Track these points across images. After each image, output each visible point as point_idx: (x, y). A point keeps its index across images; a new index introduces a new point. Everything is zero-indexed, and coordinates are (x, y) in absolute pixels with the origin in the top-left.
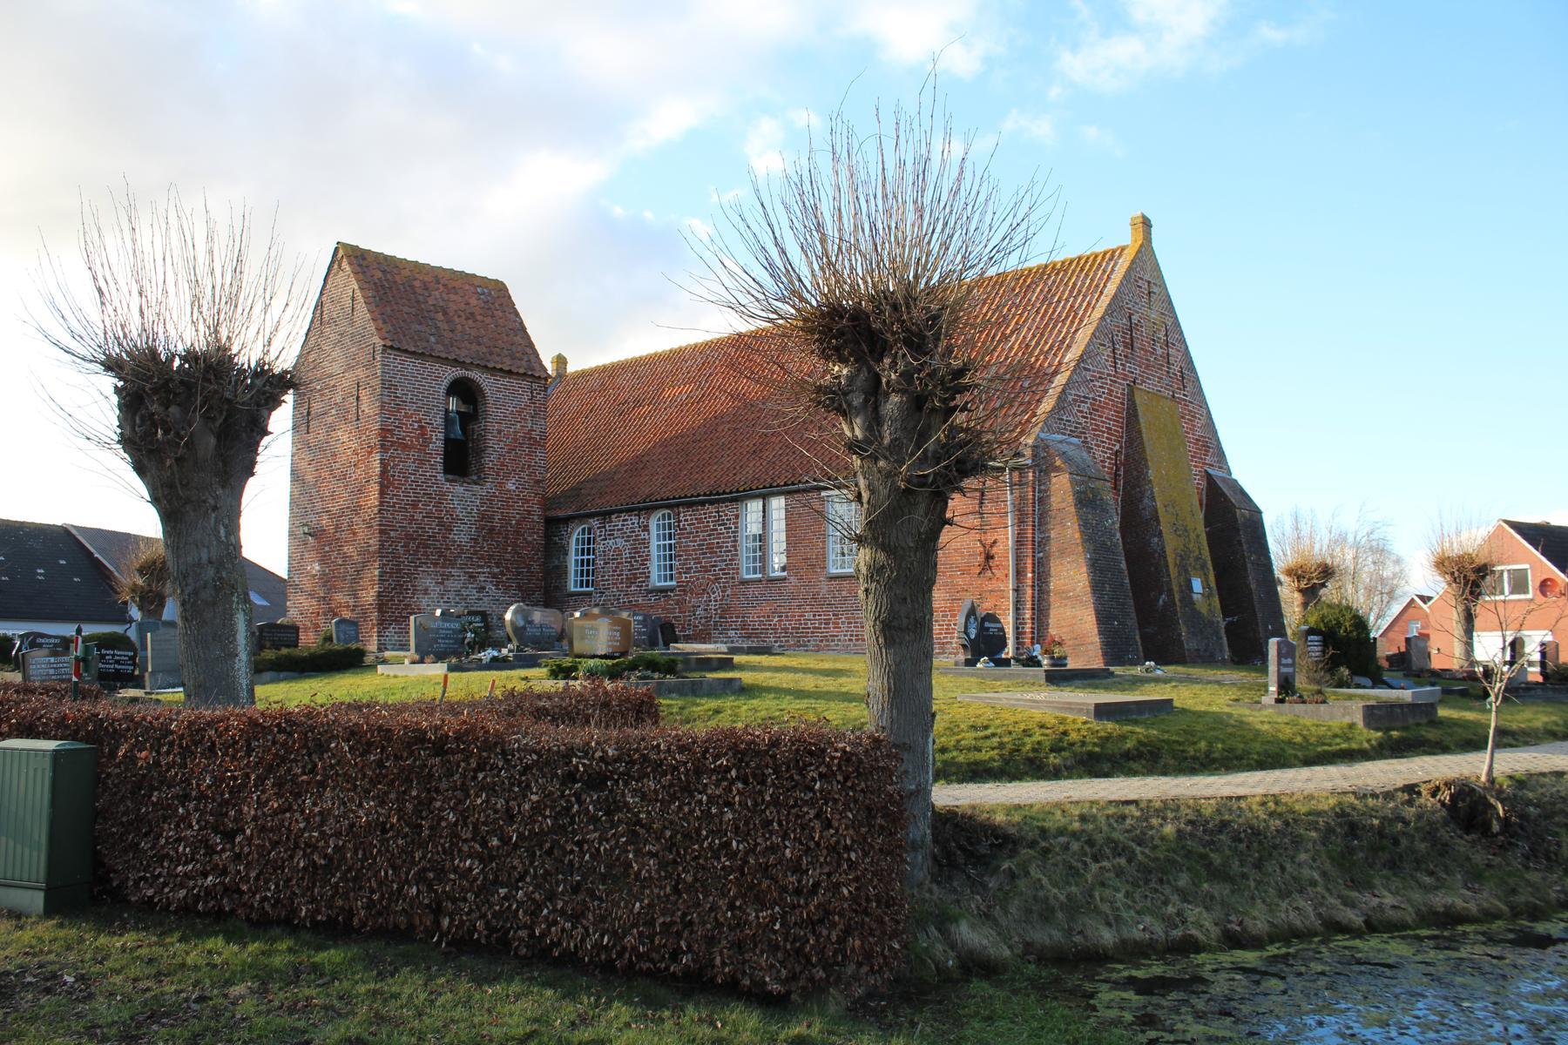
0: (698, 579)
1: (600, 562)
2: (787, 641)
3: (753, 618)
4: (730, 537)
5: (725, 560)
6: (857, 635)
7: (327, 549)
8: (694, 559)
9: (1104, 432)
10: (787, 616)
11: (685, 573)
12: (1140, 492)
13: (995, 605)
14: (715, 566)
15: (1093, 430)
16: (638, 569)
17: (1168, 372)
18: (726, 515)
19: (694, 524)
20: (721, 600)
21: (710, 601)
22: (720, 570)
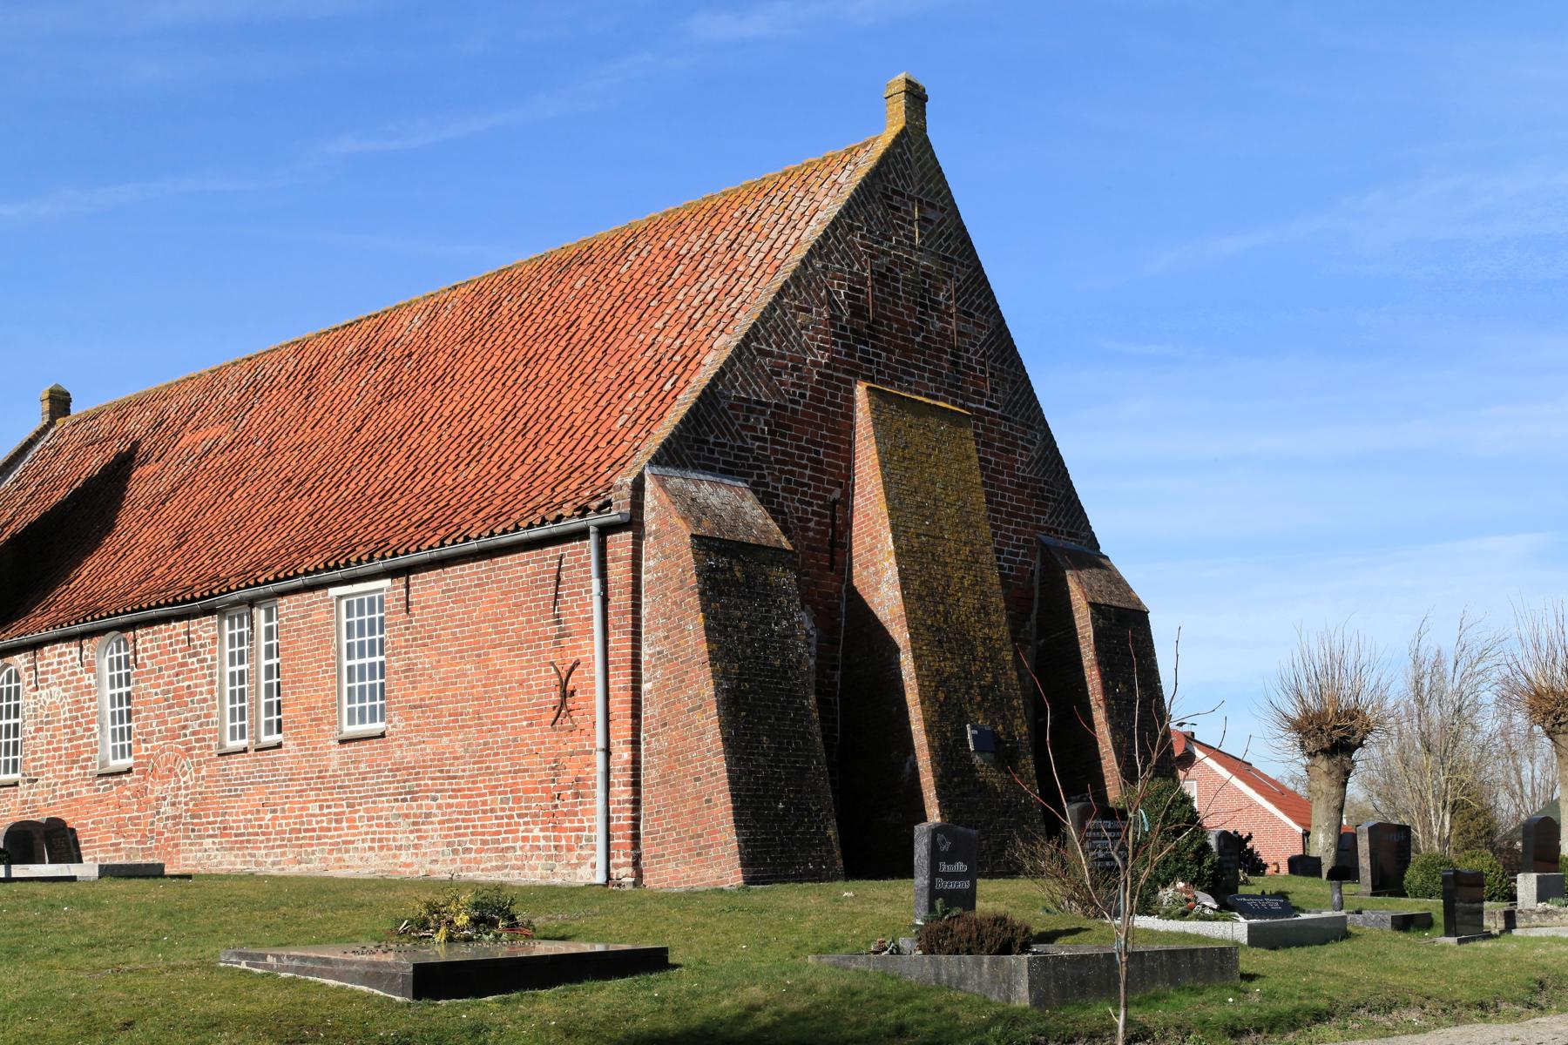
0: (163, 751)
1: (28, 728)
2: (283, 854)
3: (236, 819)
4: (204, 676)
6: (380, 840)
8: (157, 716)
9: (805, 467)
10: (283, 811)
11: (145, 741)
12: (876, 573)
13: (578, 780)
14: (185, 727)
15: (777, 461)
16: (82, 737)
17: (954, 364)
18: (199, 638)
20: (194, 786)
21: (179, 789)
22: (193, 733)
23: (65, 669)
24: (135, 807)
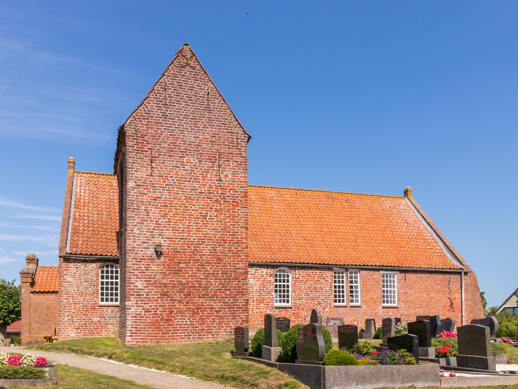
4: (328, 285)
5: (325, 296)
7: (182, 265)
14: (319, 298)
16: (266, 296)
19: (305, 277)
23: (258, 274)
24: (293, 318)
